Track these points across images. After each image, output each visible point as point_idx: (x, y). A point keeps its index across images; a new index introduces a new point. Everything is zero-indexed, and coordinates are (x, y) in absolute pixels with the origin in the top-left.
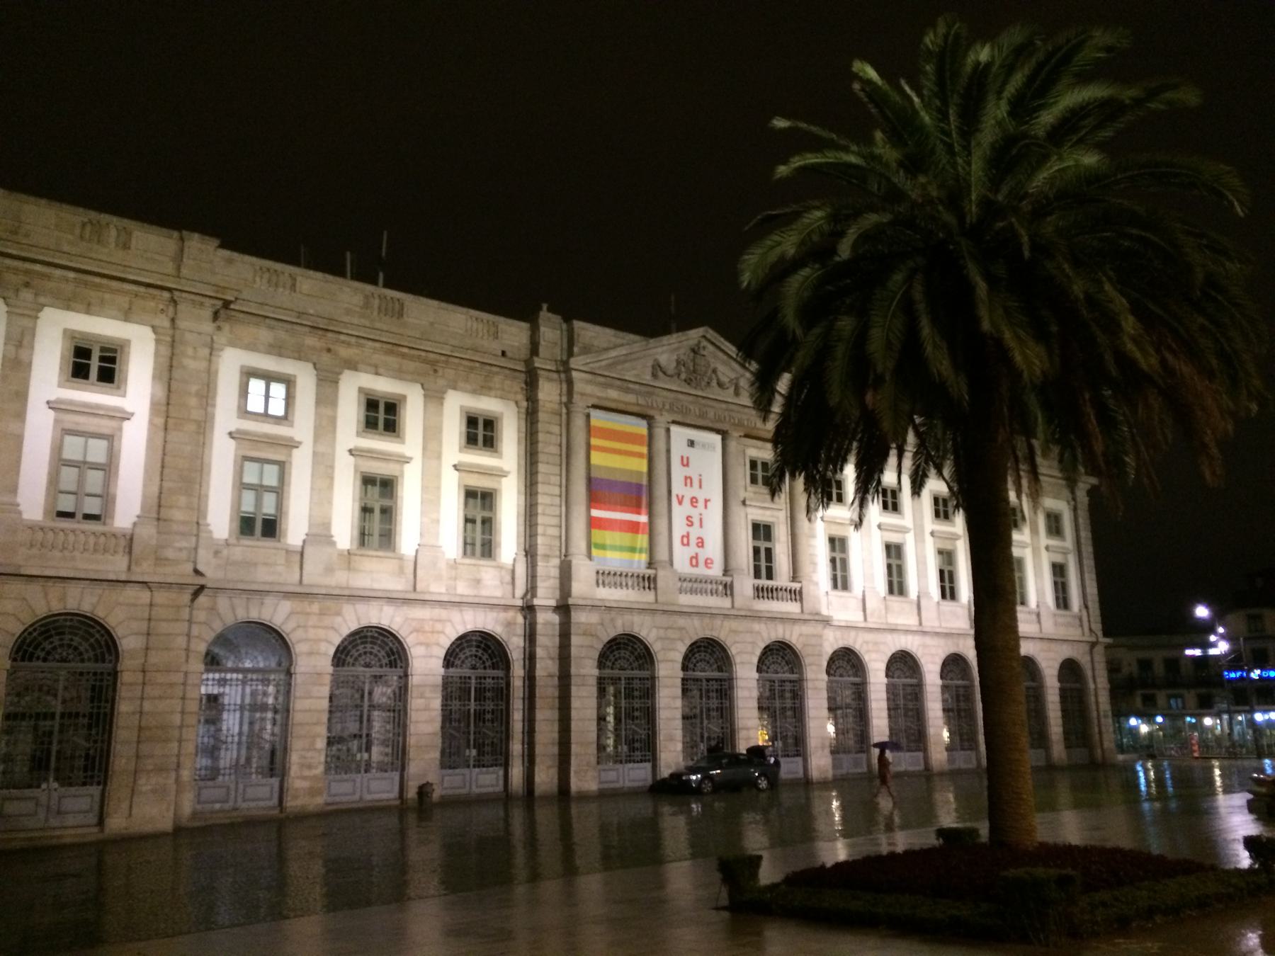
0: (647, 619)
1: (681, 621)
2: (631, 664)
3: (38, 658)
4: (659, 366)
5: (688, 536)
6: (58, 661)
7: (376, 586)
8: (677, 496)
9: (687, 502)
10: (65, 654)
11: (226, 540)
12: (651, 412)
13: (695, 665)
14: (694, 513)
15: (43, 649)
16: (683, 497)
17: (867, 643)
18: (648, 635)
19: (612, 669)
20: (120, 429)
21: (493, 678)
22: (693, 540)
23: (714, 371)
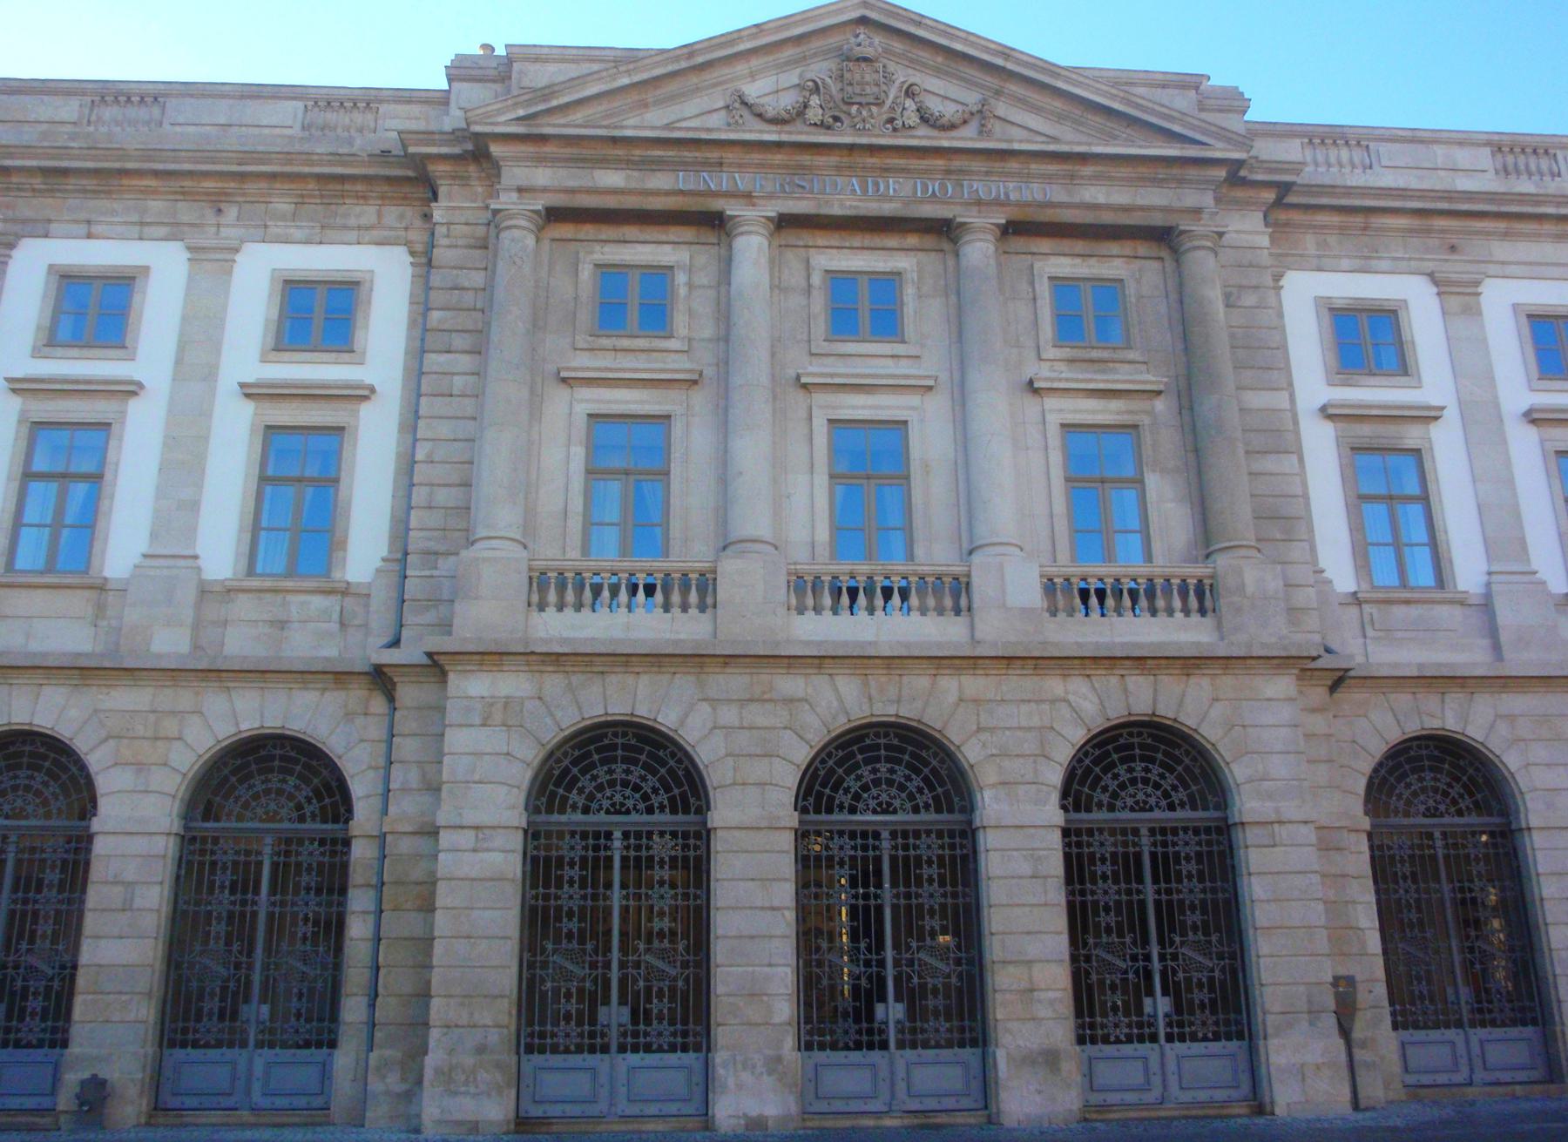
0: (683, 685)
1: (790, 684)
4: (744, 103)
7: (34, 646)
12: (717, 205)
17: (1511, 718)
18: (682, 722)
19: (586, 811)
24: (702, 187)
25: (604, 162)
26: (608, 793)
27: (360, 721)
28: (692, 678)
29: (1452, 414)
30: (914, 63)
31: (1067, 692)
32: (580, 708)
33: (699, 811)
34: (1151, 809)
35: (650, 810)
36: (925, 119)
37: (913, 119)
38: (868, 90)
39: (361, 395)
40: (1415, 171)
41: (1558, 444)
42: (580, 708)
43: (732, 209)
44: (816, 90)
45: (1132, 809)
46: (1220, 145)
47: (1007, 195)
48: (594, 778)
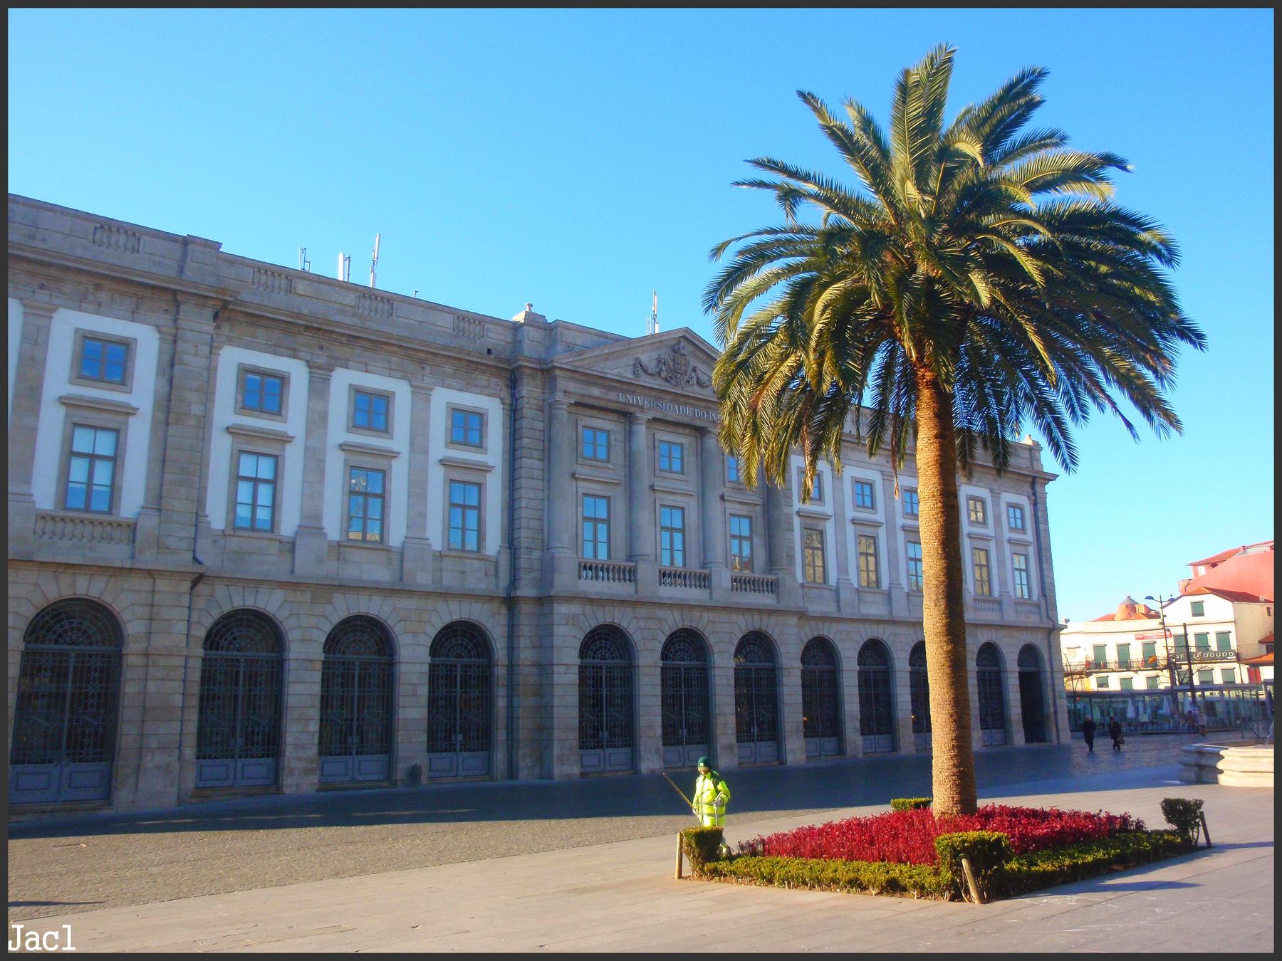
1: (660, 613)
2: (612, 653)
3: (50, 640)
6: (68, 644)
7: (365, 577)
11: (223, 531)
12: (632, 410)
13: (674, 655)
15: (54, 633)
18: (628, 626)
20: (126, 424)
21: (478, 667)
23: (694, 370)
25: (594, 384)
27: (497, 616)
28: (631, 609)
30: (695, 356)
32: (597, 619)
35: (613, 658)
37: (694, 381)
42: (597, 619)
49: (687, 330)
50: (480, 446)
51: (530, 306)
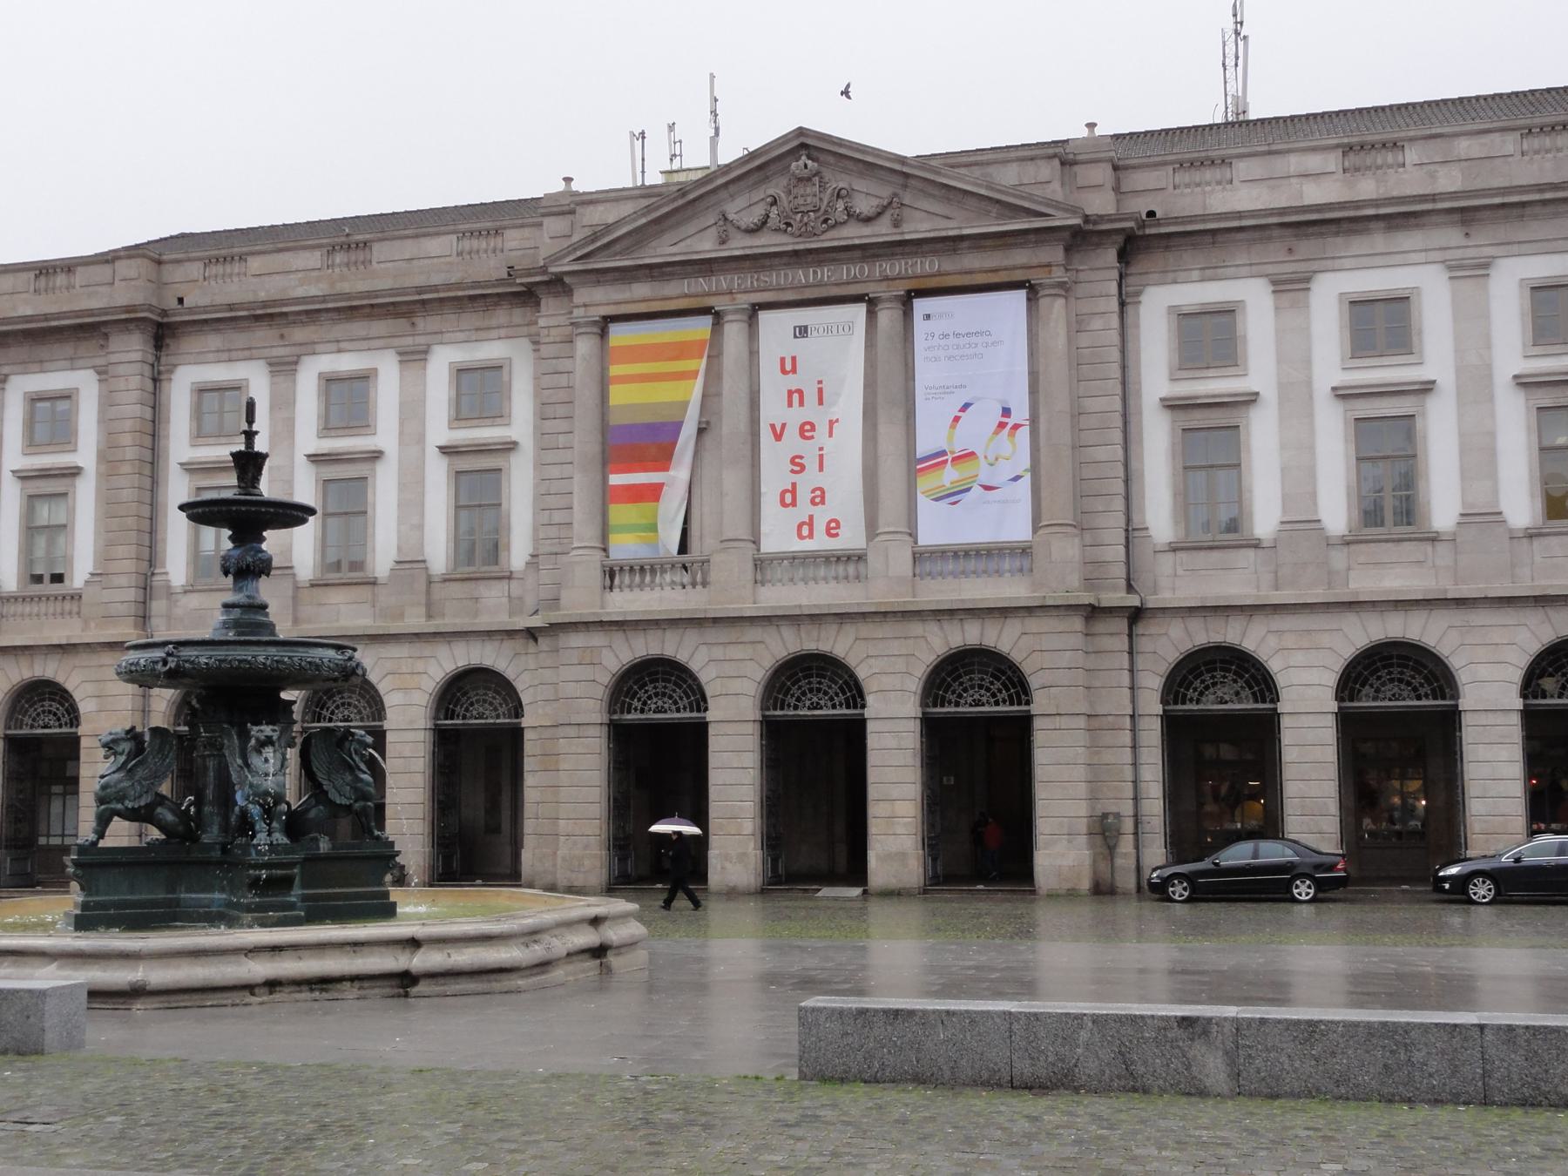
0: (692, 636)
5: (793, 491)
8: (773, 427)
9: (792, 433)
10: (46, 720)
14: (808, 450)
16: (784, 426)
19: (642, 711)
22: (804, 495)
24: (700, 289)
26: (655, 700)
29: (1269, 393)
31: (925, 631)
33: (706, 709)
34: (983, 705)
36: (850, 214)
38: (809, 200)
39: (510, 447)
40: (1268, 182)
41: (1357, 413)
43: (719, 303)
44: (774, 203)
45: (971, 705)
46: (1059, 214)
47: (906, 269)
48: (646, 692)
49: (801, 132)
50: (499, 415)
51: (568, 180)
